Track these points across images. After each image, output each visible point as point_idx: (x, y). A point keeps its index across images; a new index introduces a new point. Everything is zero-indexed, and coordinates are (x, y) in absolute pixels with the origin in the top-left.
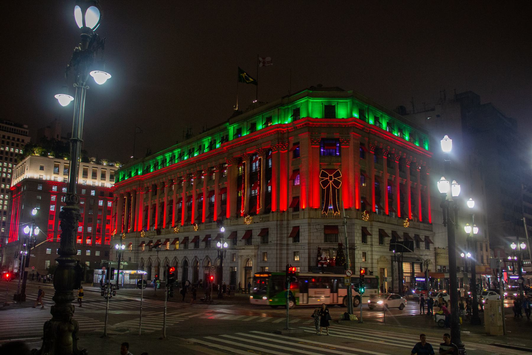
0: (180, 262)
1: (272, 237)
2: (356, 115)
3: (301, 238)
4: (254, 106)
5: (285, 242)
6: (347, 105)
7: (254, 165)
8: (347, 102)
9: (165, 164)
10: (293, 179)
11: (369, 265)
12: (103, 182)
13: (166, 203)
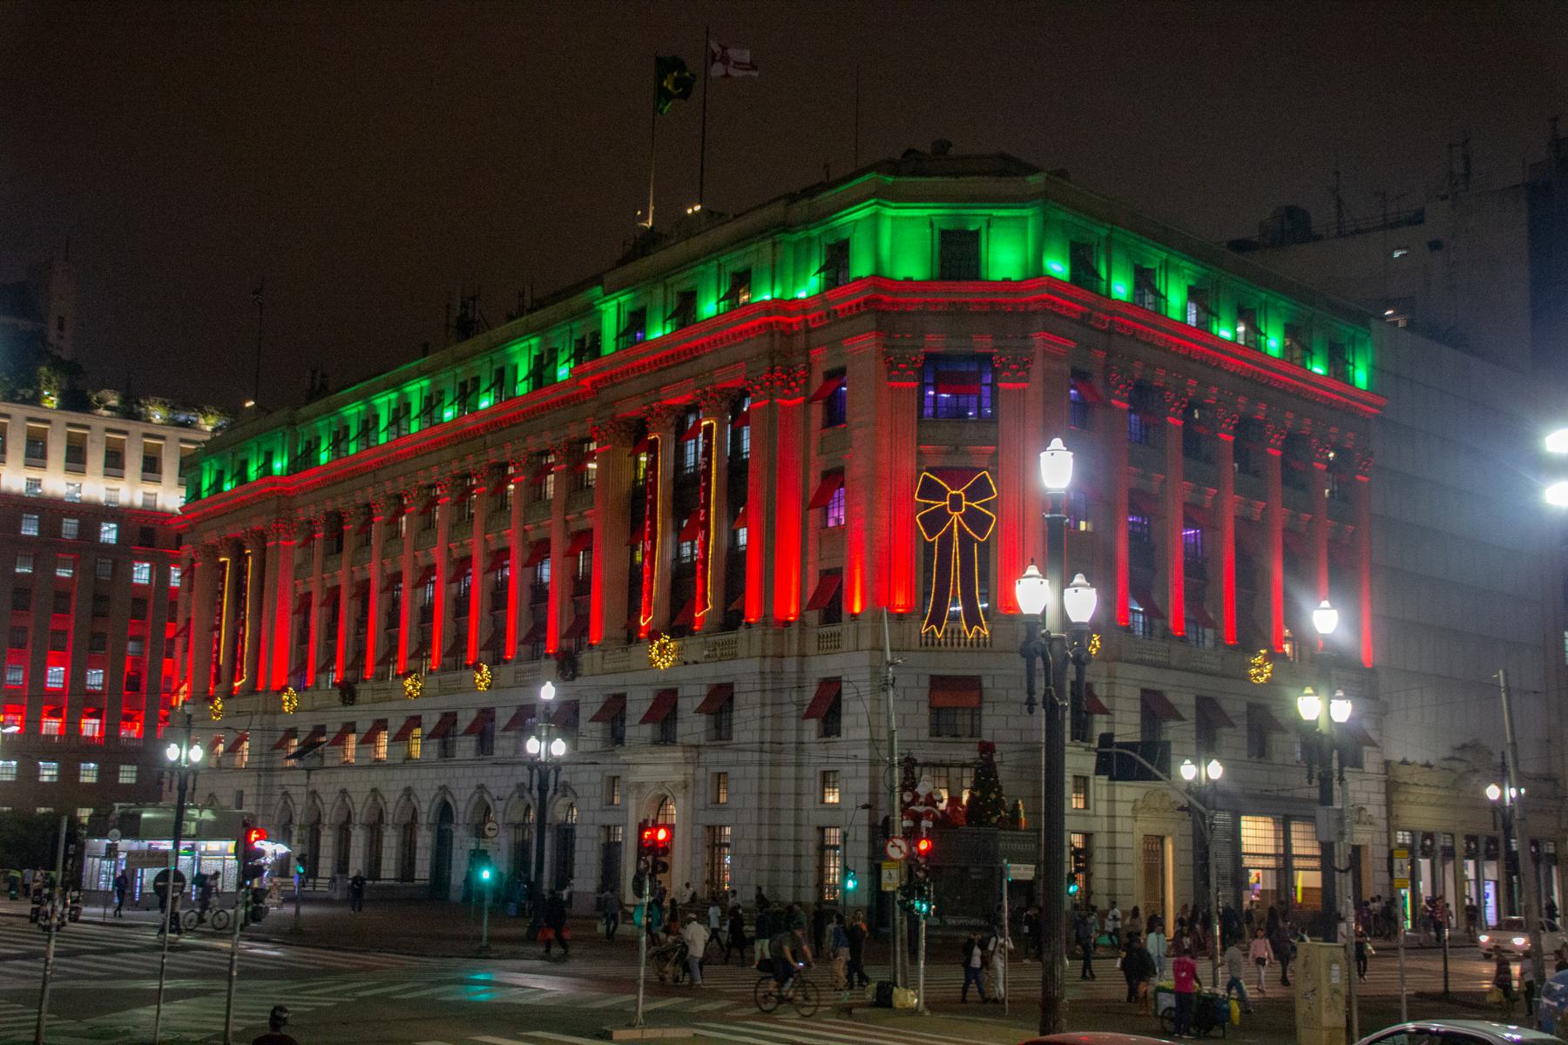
0: (425, 807)
1: (747, 722)
2: (1057, 267)
3: (846, 721)
4: (689, 228)
5: (791, 736)
6: (1026, 228)
7: (690, 449)
8: (1024, 218)
9: (372, 435)
10: (822, 501)
11: (1099, 825)
12: (151, 488)
13: (377, 585)
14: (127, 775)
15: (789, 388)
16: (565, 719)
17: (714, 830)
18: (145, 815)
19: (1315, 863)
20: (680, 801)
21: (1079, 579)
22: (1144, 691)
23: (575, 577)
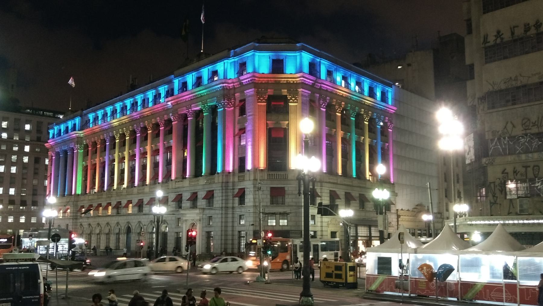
0: (123, 228)
3: (246, 200)
11: (318, 229)
14: (33, 220)
16: (164, 201)
17: (209, 233)
19: (378, 238)
23: (167, 160)
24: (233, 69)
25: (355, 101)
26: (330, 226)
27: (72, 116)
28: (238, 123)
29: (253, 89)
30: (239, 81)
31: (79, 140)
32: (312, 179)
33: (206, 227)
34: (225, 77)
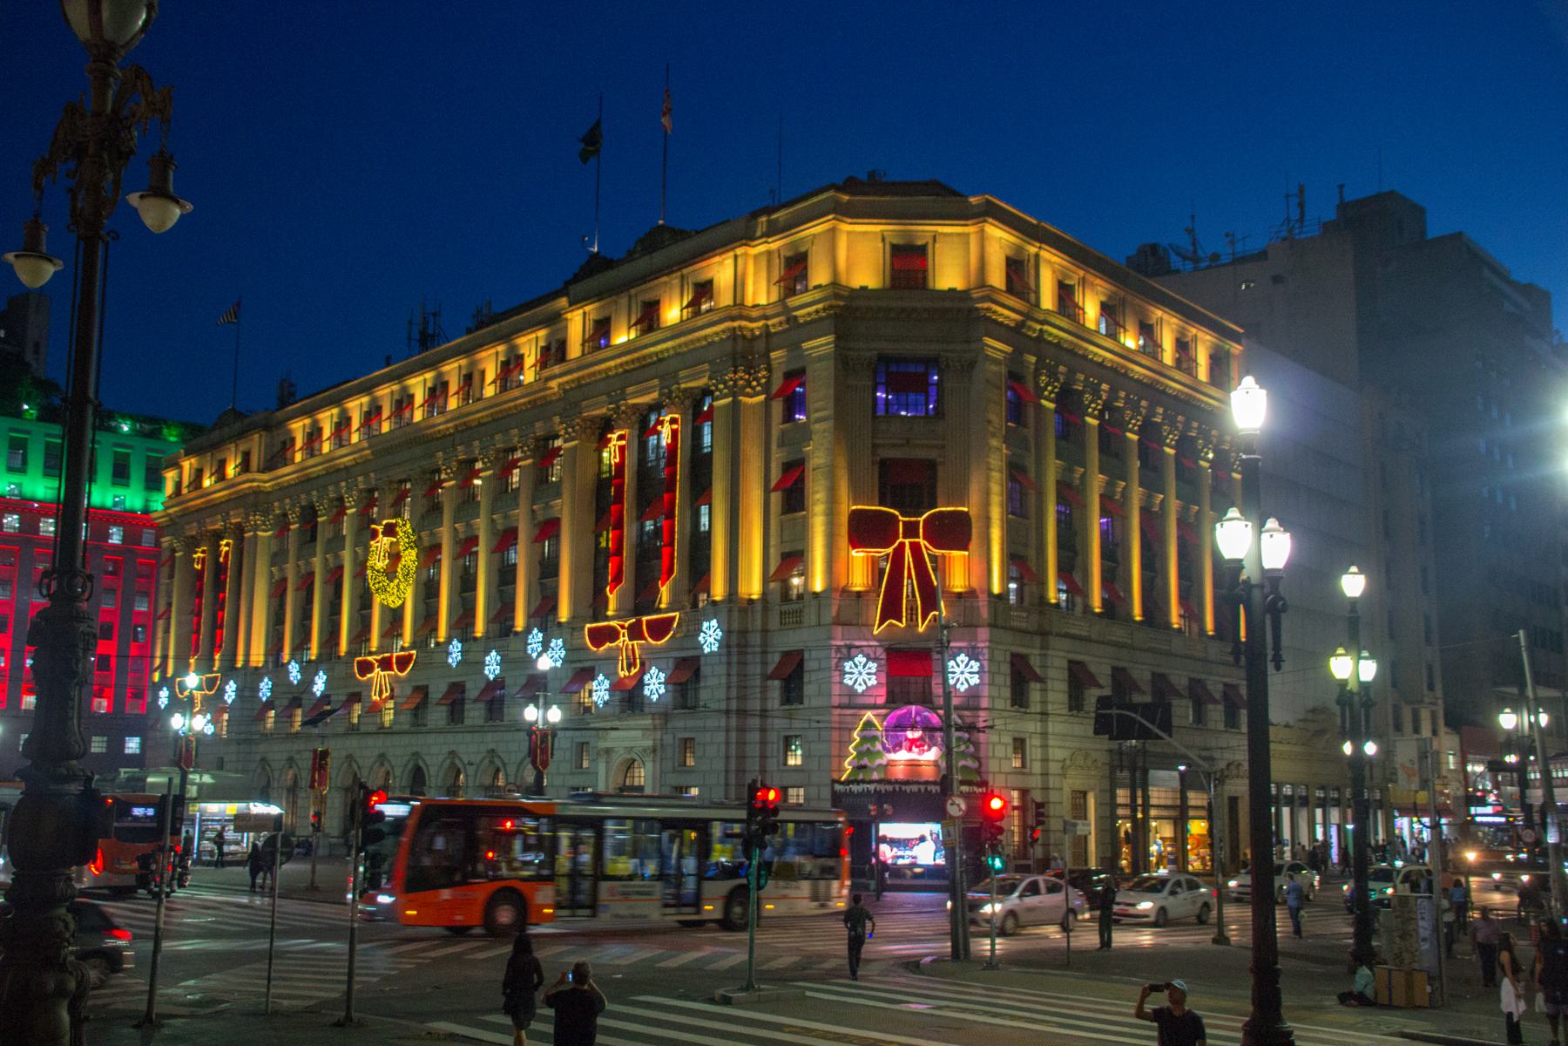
0: (398, 772)
3: (809, 689)
7: (653, 440)
8: (967, 235)
11: (1035, 782)
12: (120, 491)
15: (753, 388)
18: (150, 780)
19: (1204, 813)
20: (649, 765)
21: (1272, 523)
22: (1070, 662)
24: (764, 275)
25: (1138, 381)
26: (1071, 772)
27: (237, 426)
28: (781, 445)
29: (830, 338)
30: (785, 306)
31: (254, 501)
32: (1274, 602)
33: (674, 771)
34: (738, 303)
